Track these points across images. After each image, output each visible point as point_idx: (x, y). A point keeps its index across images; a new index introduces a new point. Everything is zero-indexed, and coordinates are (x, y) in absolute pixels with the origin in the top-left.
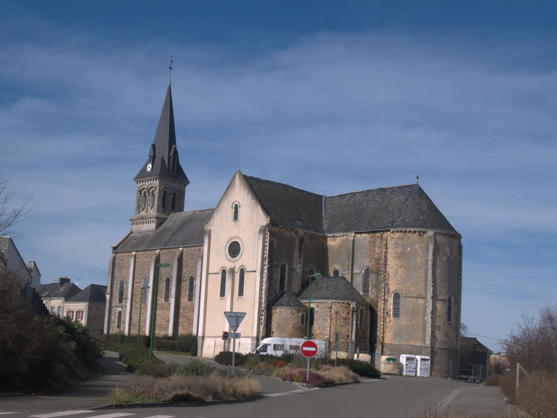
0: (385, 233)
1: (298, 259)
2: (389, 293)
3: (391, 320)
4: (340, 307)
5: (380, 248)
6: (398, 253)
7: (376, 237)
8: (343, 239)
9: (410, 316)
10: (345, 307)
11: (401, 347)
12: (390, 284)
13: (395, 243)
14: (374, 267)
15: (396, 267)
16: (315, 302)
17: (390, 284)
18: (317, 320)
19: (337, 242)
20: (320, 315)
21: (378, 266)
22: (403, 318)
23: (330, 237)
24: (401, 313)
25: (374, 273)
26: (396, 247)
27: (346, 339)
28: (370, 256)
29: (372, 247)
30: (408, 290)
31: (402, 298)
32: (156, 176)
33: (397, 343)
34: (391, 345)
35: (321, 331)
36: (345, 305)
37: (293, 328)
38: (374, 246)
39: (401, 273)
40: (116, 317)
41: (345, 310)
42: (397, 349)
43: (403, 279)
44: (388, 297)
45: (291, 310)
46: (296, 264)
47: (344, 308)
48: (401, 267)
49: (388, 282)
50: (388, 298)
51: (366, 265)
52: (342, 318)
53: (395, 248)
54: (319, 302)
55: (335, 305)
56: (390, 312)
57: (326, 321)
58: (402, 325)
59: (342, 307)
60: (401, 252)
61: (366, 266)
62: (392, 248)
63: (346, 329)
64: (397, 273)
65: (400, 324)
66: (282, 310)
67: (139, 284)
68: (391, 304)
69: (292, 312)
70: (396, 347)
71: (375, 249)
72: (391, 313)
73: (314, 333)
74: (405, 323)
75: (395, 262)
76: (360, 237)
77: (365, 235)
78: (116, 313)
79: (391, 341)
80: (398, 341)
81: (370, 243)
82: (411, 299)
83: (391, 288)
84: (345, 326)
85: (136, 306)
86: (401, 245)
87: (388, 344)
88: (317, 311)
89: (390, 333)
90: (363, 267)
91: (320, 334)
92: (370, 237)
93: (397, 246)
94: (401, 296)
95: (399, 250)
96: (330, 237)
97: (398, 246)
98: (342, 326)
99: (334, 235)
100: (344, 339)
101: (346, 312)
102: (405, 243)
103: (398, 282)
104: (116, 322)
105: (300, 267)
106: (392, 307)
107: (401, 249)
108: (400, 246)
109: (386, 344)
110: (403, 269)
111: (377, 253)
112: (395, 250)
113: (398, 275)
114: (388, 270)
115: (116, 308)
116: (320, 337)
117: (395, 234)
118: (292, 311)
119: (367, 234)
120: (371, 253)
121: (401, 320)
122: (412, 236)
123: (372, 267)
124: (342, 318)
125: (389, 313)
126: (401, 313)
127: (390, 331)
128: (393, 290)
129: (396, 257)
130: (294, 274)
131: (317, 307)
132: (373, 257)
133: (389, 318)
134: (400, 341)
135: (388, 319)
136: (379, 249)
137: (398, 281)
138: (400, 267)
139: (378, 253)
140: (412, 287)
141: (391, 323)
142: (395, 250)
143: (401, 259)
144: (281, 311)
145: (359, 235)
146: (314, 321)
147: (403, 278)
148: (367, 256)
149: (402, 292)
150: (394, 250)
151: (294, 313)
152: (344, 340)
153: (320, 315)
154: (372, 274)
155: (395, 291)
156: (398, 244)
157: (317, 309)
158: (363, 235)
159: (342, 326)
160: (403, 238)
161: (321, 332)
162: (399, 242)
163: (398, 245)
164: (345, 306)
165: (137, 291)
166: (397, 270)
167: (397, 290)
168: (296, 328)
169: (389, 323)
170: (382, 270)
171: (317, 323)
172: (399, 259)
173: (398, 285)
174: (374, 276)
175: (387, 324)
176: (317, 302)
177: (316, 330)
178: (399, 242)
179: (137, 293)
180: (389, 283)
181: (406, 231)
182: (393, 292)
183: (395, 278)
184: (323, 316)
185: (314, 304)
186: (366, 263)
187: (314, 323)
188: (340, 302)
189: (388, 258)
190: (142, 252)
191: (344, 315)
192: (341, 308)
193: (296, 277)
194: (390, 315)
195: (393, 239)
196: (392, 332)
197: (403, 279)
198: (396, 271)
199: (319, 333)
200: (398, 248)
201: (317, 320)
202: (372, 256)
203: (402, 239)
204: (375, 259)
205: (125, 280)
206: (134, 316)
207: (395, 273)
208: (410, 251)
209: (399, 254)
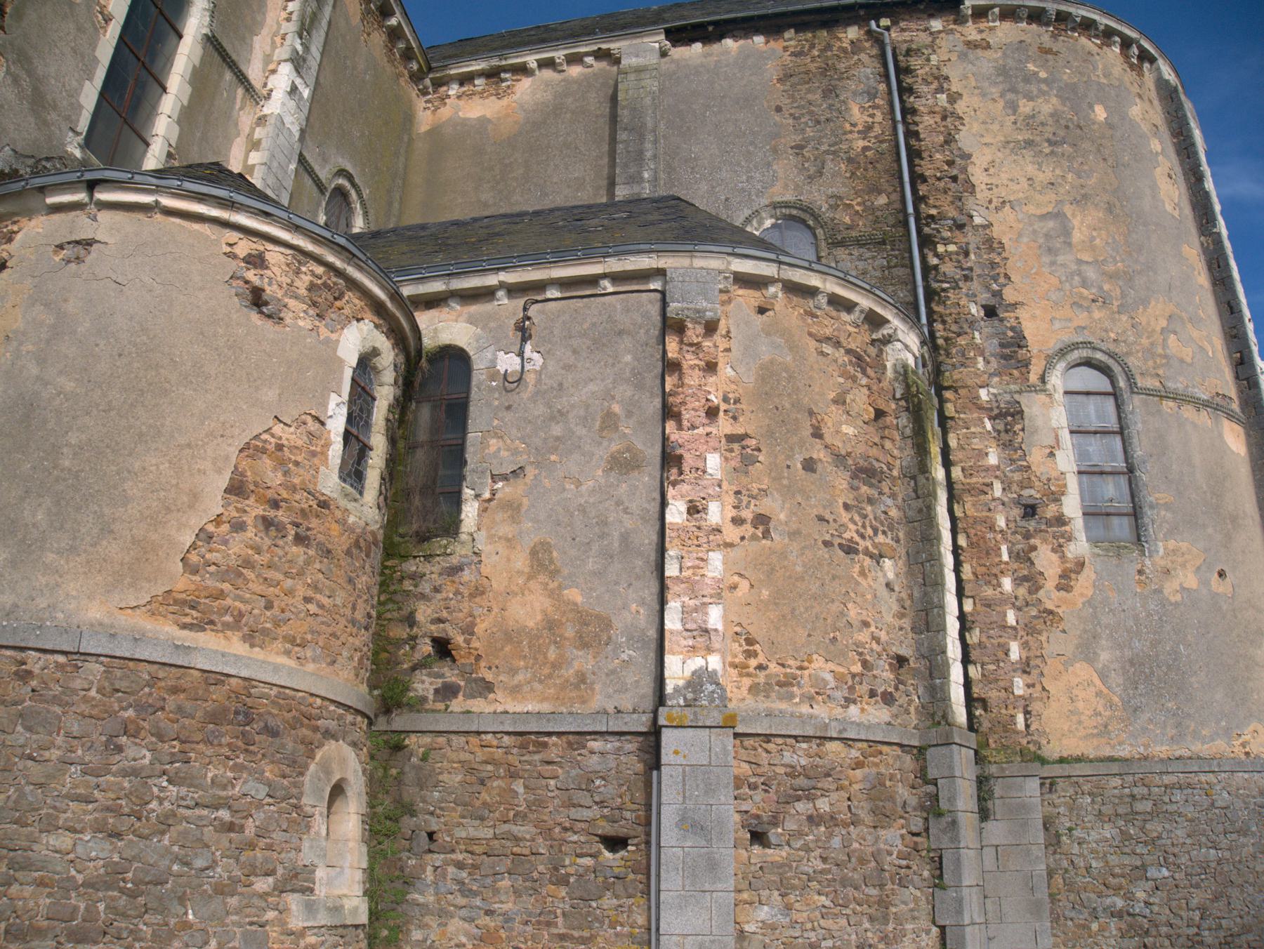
0: (902, 24)
1: (291, 27)
2: (1025, 364)
3: (1081, 565)
4: (813, 344)
5: (879, 101)
6: (1042, 124)
7: (844, 50)
8: (562, 80)
9: (1210, 530)
10: (849, 352)
11: (1203, 778)
12: (1015, 306)
13: (1003, 71)
14: (850, 206)
15: (1047, 202)
16: (491, 280)
17: (1015, 306)
18: (518, 472)
19: (515, 97)
20: (559, 416)
21: (882, 200)
22: (1172, 544)
23: (466, 79)
24: (1152, 507)
25: (859, 243)
26: (1013, 90)
27: (888, 699)
28: (799, 148)
29: (817, 96)
30: (1160, 351)
31: (1137, 399)
33: (1161, 750)
34: (1115, 768)
35: (574, 595)
36: (859, 339)
37: (237, 489)
38: (829, 92)
39: (1092, 239)
41: (854, 379)
42: (1178, 796)
43: (1112, 277)
44: (1020, 392)
45: (245, 247)
46: (268, 59)
47: (840, 355)
48: (1082, 200)
49: (998, 294)
50: (1024, 400)
51: (779, 199)
52: (840, 459)
53: (1010, 96)
54: (540, 286)
55: (762, 311)
56: (1056, 497)
57: (647, 478)
58: (1178, 598)
59: (828, 349)
60: (1055, 115)
61: (775, 206)
62: (984, 95)
63: (883, 592)
64: (1066, 232)
65: (1159, 591)
66: (105, 226)
68: (1057, 437)
69: (251, 275)
70: (1167, 779)
71: (842, 113)
72: (1072, 506)
73: (469, 631)
74: (1191, 581)
75: (1031, 169)
76: (706, 56)
77: (741, 42)
79: (1104, 730)
80: (1171, 731)
81: (795, 80)
82: (1188, 412)
83: (1029, 330)
84: (867, 552)
86: (1045, 81)
87: (1079, 760)
88: (513, 382)
89: (1082, 671)
90: (747, 212)
91: (570, 632)
92: (785, 49)
93: (1021, 86)
94: (1122, 383)
95: (1046, 109)
96: (466, 79)
97: (1034, 89)
98: (849, 549)
99: (495, 62)
100: (872, 694)
101: (860, 400)
102: (1067, 75)
103: (1085, 292)
105: (294, 90)
106: (1066, 462)
107: (1054, 100)
108: (1044, 87)
109: (1062, 760)
110: (1095, 215)
111: (860, 127)
112: (1013, 107)
113: (1070, 244)
114: (978, 220)
116: (569, 673)
117: (991, 29)
118: (257, 261)
119: (759, 40)
120: (810, 132)
121: (1157, 559)
122: (1098, 54)
123: (834, 207)
124: (840, 459)
125: (1050, 511)
126: (1152, 507)
127: (1087, 652)
128: (1053, 345)
129: (1029, 143)
130: (246, 119)
131: (514, 337)
132: (834, 153)
133: (1059, 549)
134: (1178, 725)
135: (1055, 557)
136: (875, 107)
137: (1085, 284)
138: (1075, 202)
139: (869, 128)
140: (1175, 333)
141: (1084, 583)
142: (1013, 107)
143: (1071, 159)
144: (88, 243)
145: (697, 47)
146: (468, 493)
147: (1110, 268)
148: (775, 150)
149: (1128, 354)
150: (1001, 104)
151: (270, 291)
152: (879, 714)
153: (559, 416)
154: (841, 253)
155: (1075, 346)
156: (1029, 78)
157: (508, 363)
158: (729, 42)
159: (849, 549)
160: (1048, 51)
161: (583, 618)
162: (1031, 67)
163: (1027, 80)
164: (853, 346)
166: (1058, 215)
167: (1087, 344)
168: (275, 504)
169: (1059, 588)
170: (933, 212)
171: (513, 509)
172: (1052, 152)
173: (1088, 310)
174: (860, 258)
175: (1050, 596)
176: (514, 290)
177: (498, 584)
178: (1031, 67)
180: (1009, 295)
181: (1062, 17)
182: (1062, 352)
183: (1053, 263)
184: (610, 421)
185: (475, 308)
186: (778, 188)
187: (470, 511)
188: (814, 281)
189: (967, 150)
191: (848, 430)
192: (822, 353)
193: (255, 145)
194: (1061, 520)
195: (979, 52)
196: (1104, 656)
197: (1112, 277)
198: (1051, 224)
199: (551, 625)
200: (1031, 99)
201: (518, 472)
202: (824, 148)
203: (1050, 57)
204: (850, 160)
207: (1047, 236)
208: (1109, 125)
209: (1049, 129)
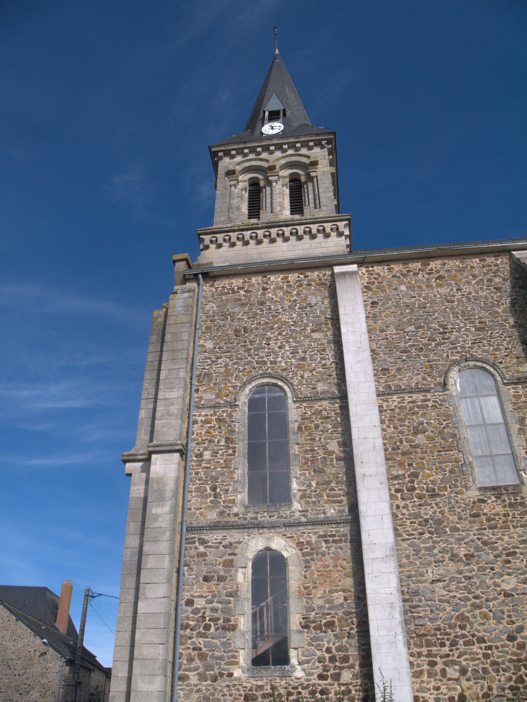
32: (317, 135)
40: (234, 594)
67: (418, 397)
78: (229, 564)
85: (427, 512)
104: (234, 628)
115: (235, 536)
165: (416, 432)
179: (420, 439)
190: (397, 268)
205: (295, 382)
206: (430, 576)
